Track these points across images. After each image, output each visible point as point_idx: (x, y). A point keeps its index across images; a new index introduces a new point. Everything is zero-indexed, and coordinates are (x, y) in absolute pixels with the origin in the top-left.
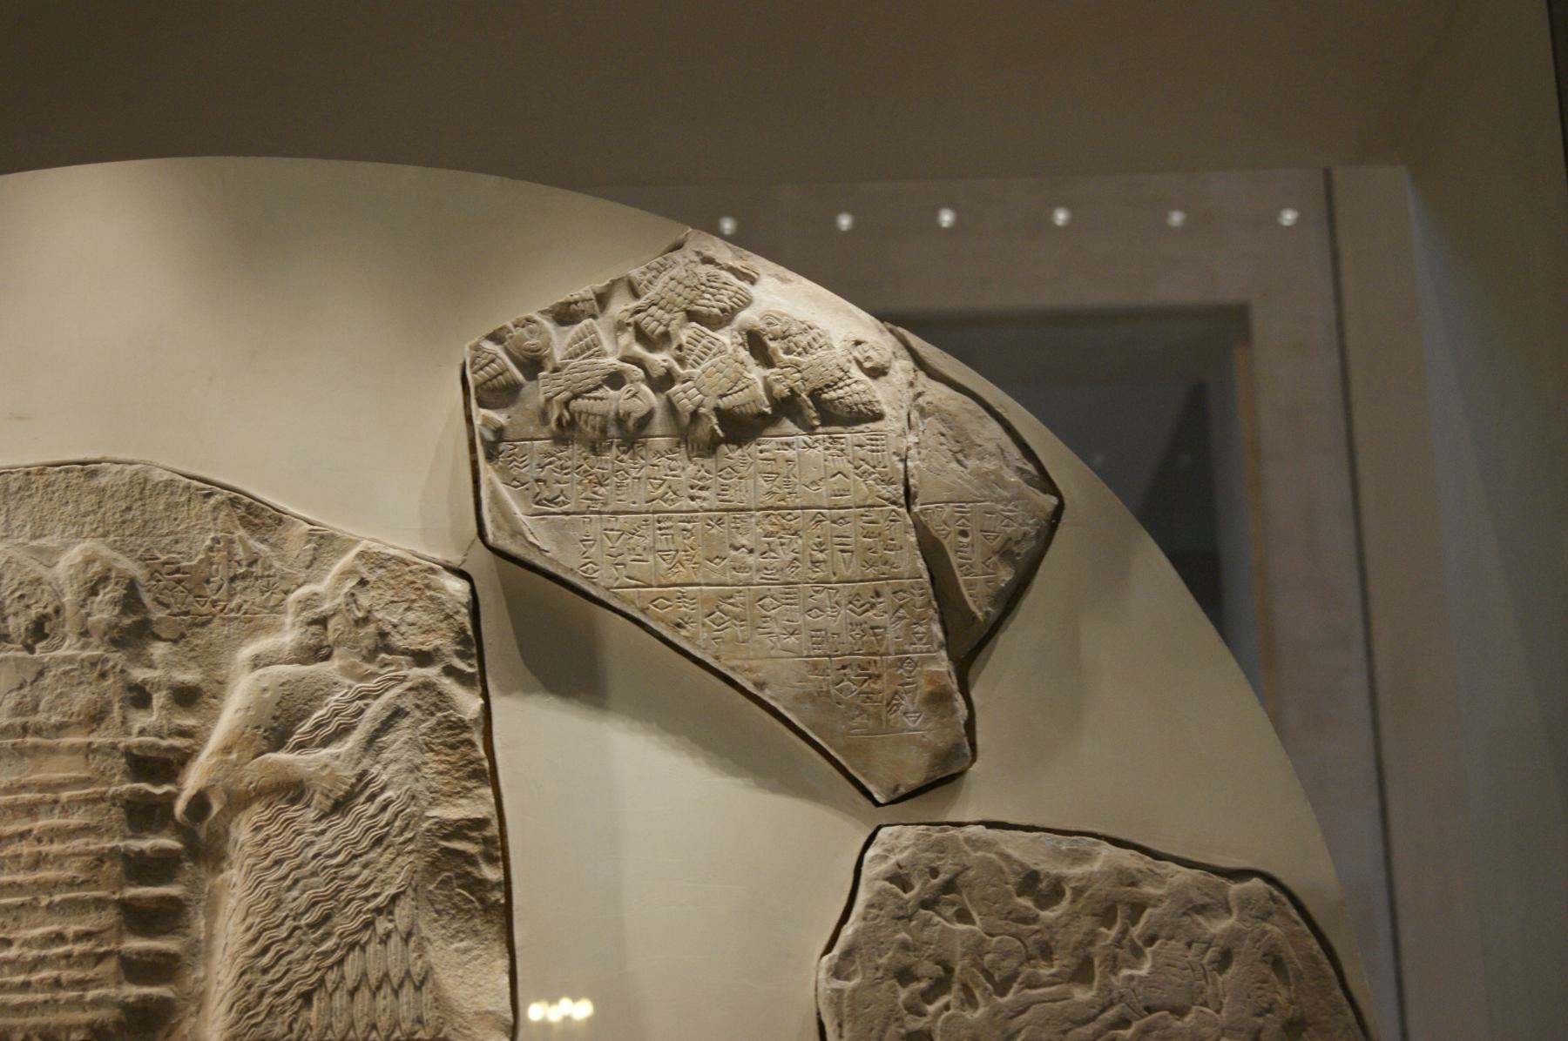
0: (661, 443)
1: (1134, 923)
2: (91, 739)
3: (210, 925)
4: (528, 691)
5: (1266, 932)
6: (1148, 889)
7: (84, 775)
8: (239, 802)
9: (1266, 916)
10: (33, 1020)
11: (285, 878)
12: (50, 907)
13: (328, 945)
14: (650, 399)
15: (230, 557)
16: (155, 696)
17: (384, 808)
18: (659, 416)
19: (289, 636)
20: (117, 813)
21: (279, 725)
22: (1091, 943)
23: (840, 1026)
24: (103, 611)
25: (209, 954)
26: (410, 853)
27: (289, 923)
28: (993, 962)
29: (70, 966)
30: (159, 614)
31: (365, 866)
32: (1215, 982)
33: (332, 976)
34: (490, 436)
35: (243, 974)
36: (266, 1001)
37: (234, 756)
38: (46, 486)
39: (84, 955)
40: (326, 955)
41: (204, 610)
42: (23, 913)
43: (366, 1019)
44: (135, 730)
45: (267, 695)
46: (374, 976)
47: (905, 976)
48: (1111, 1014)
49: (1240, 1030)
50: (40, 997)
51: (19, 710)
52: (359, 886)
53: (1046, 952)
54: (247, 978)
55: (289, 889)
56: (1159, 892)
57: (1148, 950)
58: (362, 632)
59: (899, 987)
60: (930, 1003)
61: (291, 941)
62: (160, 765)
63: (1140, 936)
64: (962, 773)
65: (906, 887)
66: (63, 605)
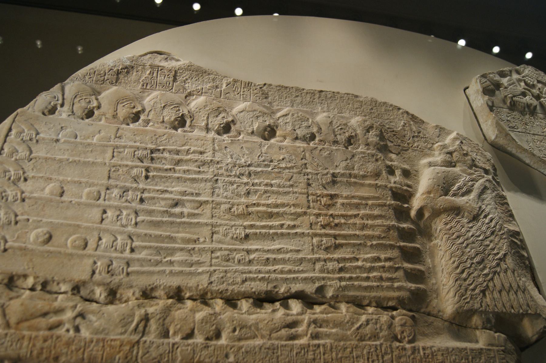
0: (541, 116)
2: (376, 182)
3: (433, 261)
4: (516, 191)
7: (376, 195)
8: (437, 213)
10: (373, 294)
11: (463, 243)
12: (372, 246)
13: (486, 272)
14: (535, 102)
15: (411, 130)
16: (396, 171)
17: (491, 221)
18: (538, 107)
19: (438, 158)
20: (391, 212)
21: (445, 186)
24: (372, 137)
25: (436, 273)
26: (505, 238)
27: (469, 261)
29: (385, 272)
30: (389, 144)
31: (491, 242)
33: (491, 284)
34: (490, 104)
35: (456, 281)
36: (469, 293)
37: (432, 195)
39: (390, 267)
40: (486, 275)
41: (406, 145)
43: (508, 304)
44: (392, 181)
45: (439, 175)
46: (507, 285)
50: (375, 284)
51: (346, 168)
52: (491, 249)
54: (459, 282)
55: (466, 247)
58: (466, 158)
61: (472, 269)
62: (403, 196)
66: (358, 134)
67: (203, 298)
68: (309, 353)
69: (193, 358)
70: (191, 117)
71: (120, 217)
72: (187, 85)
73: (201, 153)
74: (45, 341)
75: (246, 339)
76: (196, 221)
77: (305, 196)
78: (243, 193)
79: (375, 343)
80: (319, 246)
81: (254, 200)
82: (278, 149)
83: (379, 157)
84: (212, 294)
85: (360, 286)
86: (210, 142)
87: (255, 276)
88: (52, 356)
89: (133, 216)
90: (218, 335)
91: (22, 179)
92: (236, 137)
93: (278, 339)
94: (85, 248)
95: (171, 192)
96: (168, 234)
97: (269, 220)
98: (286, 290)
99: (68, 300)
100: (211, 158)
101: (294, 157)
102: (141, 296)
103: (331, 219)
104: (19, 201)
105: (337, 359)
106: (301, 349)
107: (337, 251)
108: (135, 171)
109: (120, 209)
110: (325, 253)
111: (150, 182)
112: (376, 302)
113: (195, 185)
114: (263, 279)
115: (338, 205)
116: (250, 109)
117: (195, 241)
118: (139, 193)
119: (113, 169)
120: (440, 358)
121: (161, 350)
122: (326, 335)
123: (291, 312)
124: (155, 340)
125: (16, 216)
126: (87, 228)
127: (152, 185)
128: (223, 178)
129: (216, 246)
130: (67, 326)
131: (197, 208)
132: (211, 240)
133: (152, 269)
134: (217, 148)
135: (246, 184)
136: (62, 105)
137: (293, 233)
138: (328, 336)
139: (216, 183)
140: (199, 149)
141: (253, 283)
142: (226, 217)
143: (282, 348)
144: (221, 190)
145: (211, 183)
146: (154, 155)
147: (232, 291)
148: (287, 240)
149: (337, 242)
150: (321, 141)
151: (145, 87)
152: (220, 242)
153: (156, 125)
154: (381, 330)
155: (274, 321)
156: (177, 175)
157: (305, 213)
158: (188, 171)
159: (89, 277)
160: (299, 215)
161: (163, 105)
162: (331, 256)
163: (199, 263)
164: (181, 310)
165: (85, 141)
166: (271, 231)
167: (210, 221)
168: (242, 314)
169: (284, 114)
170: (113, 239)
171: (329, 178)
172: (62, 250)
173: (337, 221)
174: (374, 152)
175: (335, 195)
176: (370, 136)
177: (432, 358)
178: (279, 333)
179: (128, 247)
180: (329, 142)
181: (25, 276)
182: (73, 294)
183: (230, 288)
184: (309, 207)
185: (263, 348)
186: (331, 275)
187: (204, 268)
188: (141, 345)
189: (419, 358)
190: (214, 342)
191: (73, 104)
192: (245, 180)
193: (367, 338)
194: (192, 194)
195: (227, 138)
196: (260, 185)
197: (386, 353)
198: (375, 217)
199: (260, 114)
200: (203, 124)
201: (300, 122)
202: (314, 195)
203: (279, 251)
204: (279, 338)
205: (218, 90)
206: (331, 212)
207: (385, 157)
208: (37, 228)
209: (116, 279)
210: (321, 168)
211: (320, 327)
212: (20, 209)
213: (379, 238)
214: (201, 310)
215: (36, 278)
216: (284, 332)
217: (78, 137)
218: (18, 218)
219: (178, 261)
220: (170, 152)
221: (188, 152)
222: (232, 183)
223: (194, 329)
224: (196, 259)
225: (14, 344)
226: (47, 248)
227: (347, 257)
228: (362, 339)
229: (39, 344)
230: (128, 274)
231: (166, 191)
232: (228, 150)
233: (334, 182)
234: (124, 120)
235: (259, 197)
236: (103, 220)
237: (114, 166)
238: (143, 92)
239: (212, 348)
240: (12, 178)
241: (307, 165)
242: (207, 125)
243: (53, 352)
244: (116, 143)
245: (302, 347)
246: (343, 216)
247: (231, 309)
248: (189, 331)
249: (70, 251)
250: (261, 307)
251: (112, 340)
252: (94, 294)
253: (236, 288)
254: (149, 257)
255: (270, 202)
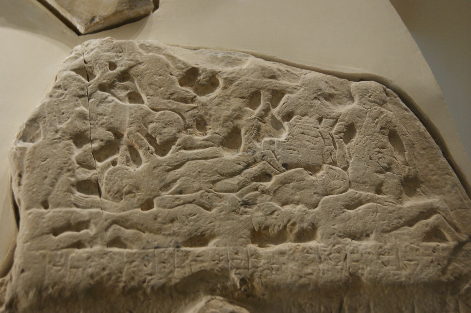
1: (275, 106)
5: (382, 113)
6: (284, 82)
9: (382, 103)
22: (238, 117)
23: (20, 176)
28: (155, 129)
32: (341, 147)
47: (79, 138)
48: (254, 169)
49: (364, 183)
53: (201, 124)
56: (294, 84)
57: (285, 124)
59: (74, 147)
60: (100, 161)
63: (279, 112)
64: (146, 15)
65: (89, 75)
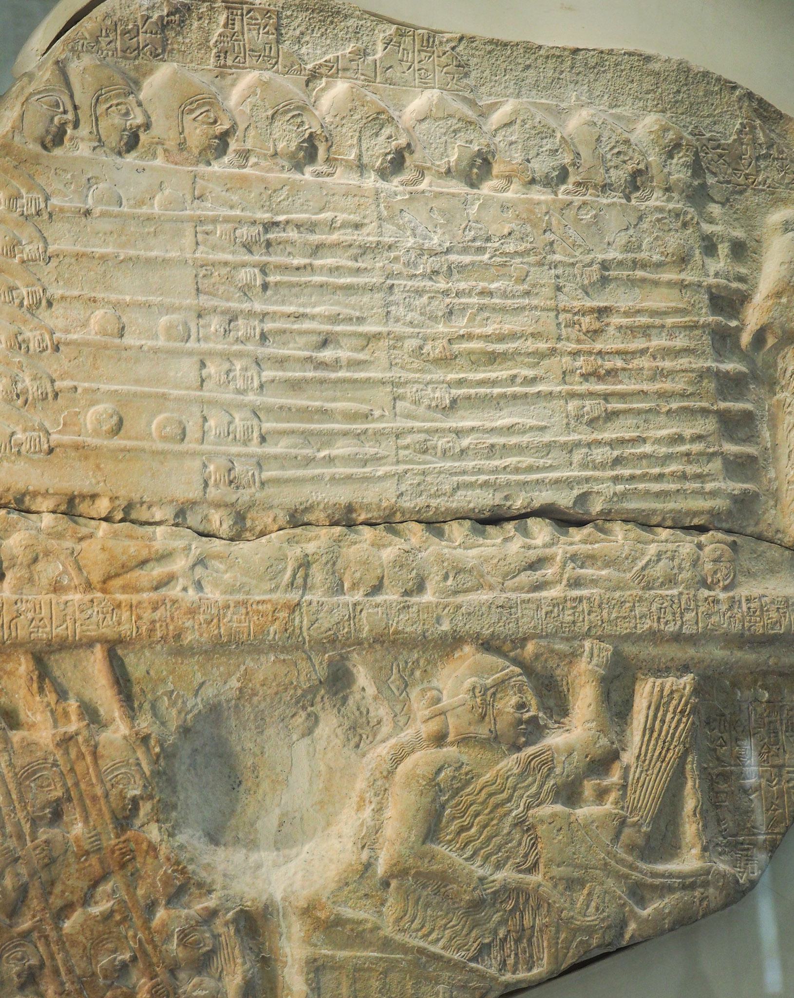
2: (682, 276)
3: (774, 436)
7: (681, 306)
10: (671, 505)
15: (754, 140)
20: (707, 339)
24: (678, 171)
25: (776, 459)
29: (690, 462)
30: (711, 180)
38: (616, 65)
39: (701, 454)
41: (741, 180)
42: (651, 417)
44: (712, 273)
50: (673, 487)
51: (628, 248)
62: (728, 302)
67: (389, 521)
68: (566, 612)
69: (387, 627)
70: (327, 140)
71: (231, 375)
72: (304, 50)
73: (357, 226)
74: (155, 609)
75: (466, 591)
76: (363, 375)
77: (552, 314)
78: (440, 314)
79: (669, 592)
80: (578, 417)
81: (461, 328)
82: (499, 210)
83: (689, 216)
84: (403, 513)
85: (647, 492)
86: (371, 200)
87: (473, 479)
88: (171, 635)
89: (253, 372)
90: (420, 587)
91: (44, 302)
92: (415, 183)
93: (514, 590)
94: (183, 440)
95: (313, 317)
96: (318, 404)
97: (490, 368)
98: (525, 504)
99: (173, 536)
100: (376, 239)
101: (529, 229)
102: (288, 522)
103: (600, 362)
104: (49, 351)
105: (609, 621)
106: (554, 606)
107: (609, 424)
108: (244, 275)
109: (228, 357)
110: (589, 429)
111: (272, 296)
112: (673, 519)
113: (353, 300)
114: (485, 484)
115: (611, 330)
116: (441, 115)
117: (366, 417)
118: (257, 323)
119: (203, 272)
120: (774, 615)
121: (336, 618)
122: (592, 581)
123: (533, 542)
124: (323, 599)
125: (53, 381)
126: (178, 399)
127: (276, 303)
128: (403, 282)
129: (403, 425)
130: (181, 582)
131: (363, 349)
132: (392, 413)
133: (300, 473)
134: (385, 213)
135: (446, 293)
136: (76, 125)
137: (533, 394)
138: (594, 582)
139: (391, 294)
140: (352, 217)
141: (470, 493)
142: (415, 366)
143: (524, 606)
144: (402, 311)
145: (381, 295)
146: (270, 236)
147: (437, 508)
148: (523, 407)
149: (610, 407)
150: (579, 184)
151: (222, 62)
152: (408, 416)
153: (263, 163)
154: (681, 569)
155: (509, 560)
156: (317, 279)
157: (553, 352)
158: (337, 268)
159: (201, 494)
160: (541, 356)
161: (270, 112)
162: (600, 437)
163: (377, 459)
164: (357, 546)
165: (138, 211)
166: (497, 391)
167: (388, 375)
168: (455, 548)
169: (507, 121)
170: (227, 418)
171: (594, 272)
172: (145, 444)
173: (608, 365)
174: (680, 206)
175: (606, 308)
176: (673, 167)
177: (761, 616)
178: (517, 579)
179: (256, 434)
180: (595, 186)
181: (94, 497)
182: (177, 525)
183: (434, 503)
184: (559, 339)
185: (494, 606)
186: (597, 473)
187: (388, 468)
188: (304, 609)
189: (739, 616)
190: (415, 599)
191: (97, 120)
192: (442, 285)
193: (657, 584)
194: (351, 319)
195: (401, 188)
196: (470, 294)
197: (687, 609)
198: (677, 353)
199: (460, 125)
200: (352, 157)
201: (538, 141)
202: (569, 311)
203: (510, 430)
204: (518, 589)
205: (370, 58)
206: (598, 346)
207: (700, 214)
208: (93, 403)
209: (245, 495)
210: (581, 250)
211: (582, 567)
212: (55, 367)
213: (683, 395)
214: (390, 544)
215: (112, 499)
216: (525, 578)
217: (124, 202)
218: (58, 384)
219: (343, 458)
220: (298, 226)
221: (331, 226)
222: (419, 292)
223: (383, 577)
224: (373, 451)
225: (108, 616)
226: (118, 442)
227: (627, 436)
228: (648, 587)
229: (147, 615)
230: (263, 484)
231: (304, 315)
232: (407, 217)
233: (604, 281)
234: (200, 153)
235: (469, 320)
236: (203, 381)
237: (202, 266)
238: (221, 75)
239: (415, 609)
240: (26, 303)
241: (555, 246)
242: (360, 157)
243: (171, 628)
244: (199, 212)
245: (555, 603)
246: (618, 353)
247: (437, 540)
248: (375, 582)
249: (160, 446)
250: (483, 534)
251: (258, 602)
252: (209, 521)
253: (441, 503)
254: (294, 451)
255: (489, 330)
